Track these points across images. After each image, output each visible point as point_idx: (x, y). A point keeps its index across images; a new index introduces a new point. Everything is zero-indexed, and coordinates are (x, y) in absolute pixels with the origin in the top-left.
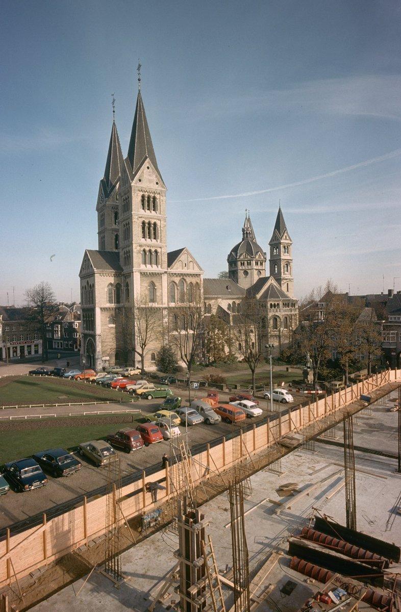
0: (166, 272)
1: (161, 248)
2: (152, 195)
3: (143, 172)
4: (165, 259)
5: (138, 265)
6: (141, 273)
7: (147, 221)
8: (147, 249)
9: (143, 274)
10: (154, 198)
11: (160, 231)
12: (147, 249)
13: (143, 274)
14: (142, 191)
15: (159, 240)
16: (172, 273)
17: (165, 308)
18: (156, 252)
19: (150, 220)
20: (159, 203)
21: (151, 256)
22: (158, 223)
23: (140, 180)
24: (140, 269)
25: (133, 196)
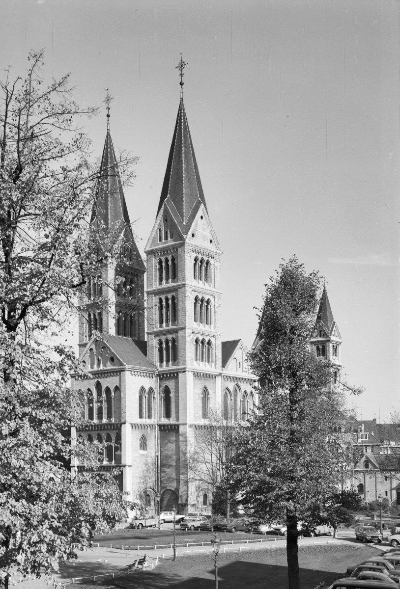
0: (220, 374)
1: (214, 337)
2: (206, 258)
3: (197, 224)
4: (217, 352)
5: (190, 360)
6: (194, 374)
7: (200, 297)
8: (201, 338)
9: (196, 375)
10: (208, 263)
11: (213, 313)
12: (201, 338)
13: (196, 375)
14: (195, 251)
15: (213, 326)
16: (227, 377)
17: (220, 428)
18: (209, 343)
19: (204, 295)
20: (212, 271)
21: (204, 345)
22: (212, 299)
23: (193, 235)
24: (193, 367)
25: (186, 258)
